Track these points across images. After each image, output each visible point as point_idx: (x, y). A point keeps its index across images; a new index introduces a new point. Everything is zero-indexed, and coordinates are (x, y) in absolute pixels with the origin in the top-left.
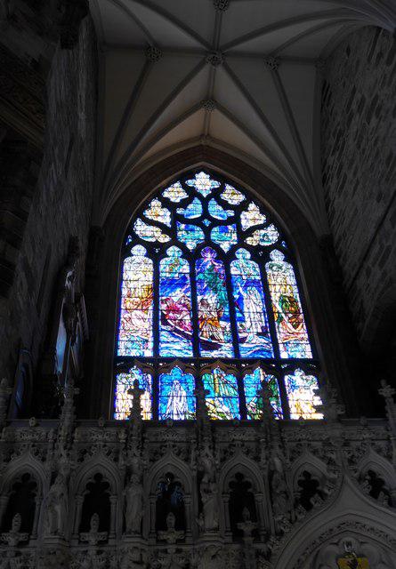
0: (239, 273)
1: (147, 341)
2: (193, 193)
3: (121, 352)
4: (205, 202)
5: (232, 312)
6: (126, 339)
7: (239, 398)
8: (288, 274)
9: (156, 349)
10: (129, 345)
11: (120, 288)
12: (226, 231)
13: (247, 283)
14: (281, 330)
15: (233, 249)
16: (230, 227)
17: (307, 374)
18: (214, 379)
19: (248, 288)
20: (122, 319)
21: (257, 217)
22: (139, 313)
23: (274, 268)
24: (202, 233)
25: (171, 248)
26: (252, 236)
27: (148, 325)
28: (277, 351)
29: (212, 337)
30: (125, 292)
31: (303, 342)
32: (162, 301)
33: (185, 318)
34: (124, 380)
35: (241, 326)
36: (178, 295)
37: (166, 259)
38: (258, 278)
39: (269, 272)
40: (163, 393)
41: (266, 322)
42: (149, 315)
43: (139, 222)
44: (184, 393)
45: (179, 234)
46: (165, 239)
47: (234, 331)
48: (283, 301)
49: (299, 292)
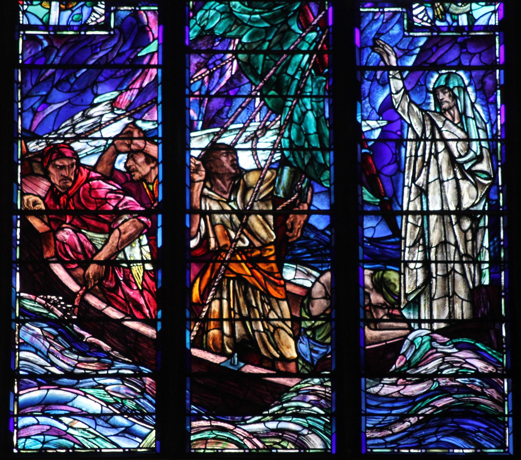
19: (433, 80)
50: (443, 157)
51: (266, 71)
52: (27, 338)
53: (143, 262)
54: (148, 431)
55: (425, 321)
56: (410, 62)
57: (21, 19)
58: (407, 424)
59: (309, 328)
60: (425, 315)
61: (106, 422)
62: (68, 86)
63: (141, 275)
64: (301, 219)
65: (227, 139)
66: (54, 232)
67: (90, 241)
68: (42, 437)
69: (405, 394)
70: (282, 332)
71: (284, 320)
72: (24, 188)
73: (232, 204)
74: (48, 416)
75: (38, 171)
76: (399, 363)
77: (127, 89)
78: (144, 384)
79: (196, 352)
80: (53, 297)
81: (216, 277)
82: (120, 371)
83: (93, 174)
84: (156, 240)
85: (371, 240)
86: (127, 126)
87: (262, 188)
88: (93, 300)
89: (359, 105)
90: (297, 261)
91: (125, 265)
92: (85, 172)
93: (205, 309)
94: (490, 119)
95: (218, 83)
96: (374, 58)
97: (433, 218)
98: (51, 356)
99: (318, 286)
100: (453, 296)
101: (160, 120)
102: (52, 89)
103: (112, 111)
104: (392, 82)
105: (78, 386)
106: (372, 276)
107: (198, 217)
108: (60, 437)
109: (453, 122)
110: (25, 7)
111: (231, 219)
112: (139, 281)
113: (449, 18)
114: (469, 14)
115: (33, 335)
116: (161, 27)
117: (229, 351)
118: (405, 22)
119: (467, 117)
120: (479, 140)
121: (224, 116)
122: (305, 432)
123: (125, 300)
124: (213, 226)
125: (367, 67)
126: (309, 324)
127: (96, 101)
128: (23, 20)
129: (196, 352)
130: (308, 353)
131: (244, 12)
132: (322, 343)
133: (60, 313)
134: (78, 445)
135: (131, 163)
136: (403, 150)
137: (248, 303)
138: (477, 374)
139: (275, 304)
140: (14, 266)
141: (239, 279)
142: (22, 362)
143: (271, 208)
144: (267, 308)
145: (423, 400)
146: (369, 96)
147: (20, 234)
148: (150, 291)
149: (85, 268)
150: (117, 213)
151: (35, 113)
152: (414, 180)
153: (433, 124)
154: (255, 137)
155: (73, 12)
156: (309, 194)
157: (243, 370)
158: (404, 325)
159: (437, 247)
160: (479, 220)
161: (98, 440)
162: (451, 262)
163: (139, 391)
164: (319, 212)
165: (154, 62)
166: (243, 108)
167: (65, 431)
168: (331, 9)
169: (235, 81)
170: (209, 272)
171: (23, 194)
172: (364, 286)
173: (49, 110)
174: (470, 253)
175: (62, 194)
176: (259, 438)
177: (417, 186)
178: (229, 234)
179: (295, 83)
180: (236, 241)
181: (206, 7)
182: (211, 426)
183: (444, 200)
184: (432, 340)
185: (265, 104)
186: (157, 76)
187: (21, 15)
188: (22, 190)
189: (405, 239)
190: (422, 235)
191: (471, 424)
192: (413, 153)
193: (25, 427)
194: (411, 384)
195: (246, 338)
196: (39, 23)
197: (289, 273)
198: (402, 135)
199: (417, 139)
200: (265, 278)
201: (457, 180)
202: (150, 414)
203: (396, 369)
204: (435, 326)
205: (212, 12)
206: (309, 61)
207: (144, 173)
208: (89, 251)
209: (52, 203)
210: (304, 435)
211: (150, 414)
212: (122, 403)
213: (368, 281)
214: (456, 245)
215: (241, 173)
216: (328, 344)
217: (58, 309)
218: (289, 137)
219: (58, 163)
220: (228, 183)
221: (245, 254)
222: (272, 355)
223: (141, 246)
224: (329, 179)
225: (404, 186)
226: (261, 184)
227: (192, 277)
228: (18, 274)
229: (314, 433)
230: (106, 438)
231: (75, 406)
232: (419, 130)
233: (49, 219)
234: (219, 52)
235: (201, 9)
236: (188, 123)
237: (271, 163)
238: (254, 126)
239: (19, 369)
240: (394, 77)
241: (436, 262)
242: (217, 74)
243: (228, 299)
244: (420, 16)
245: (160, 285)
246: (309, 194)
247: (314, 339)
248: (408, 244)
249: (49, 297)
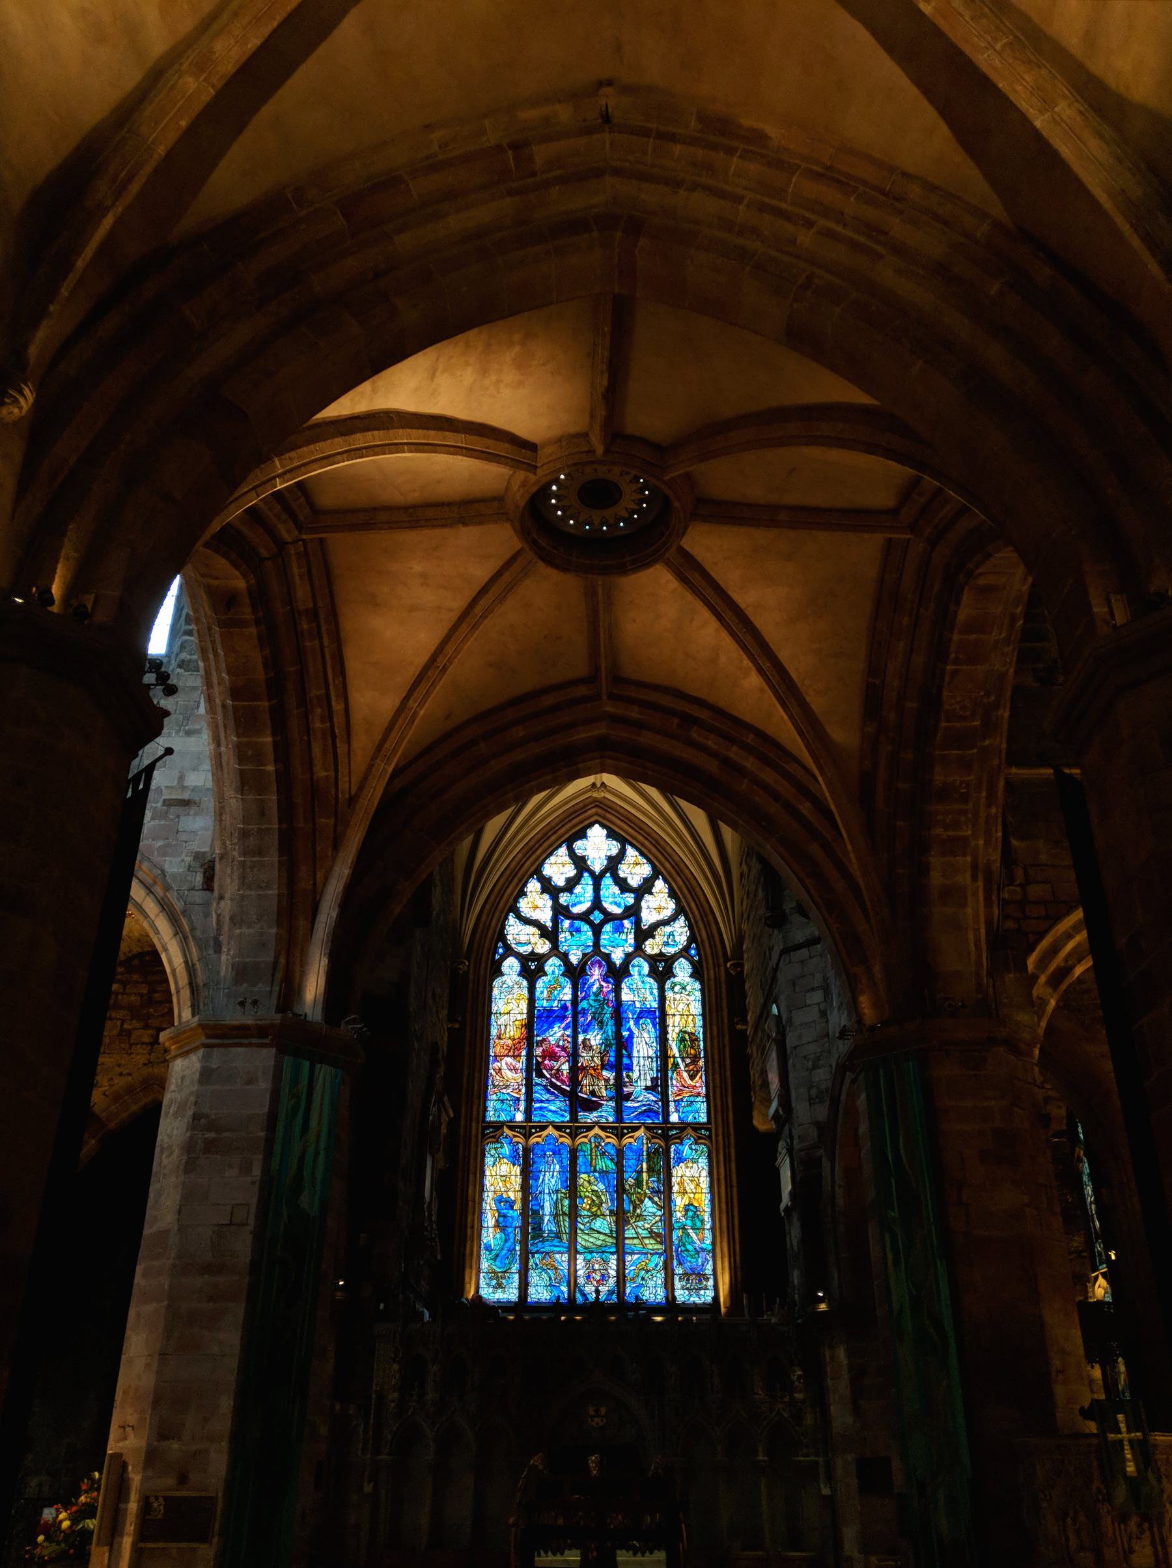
1: (518, 1099)
2: (580, 863)
3: (491, 1116)
4: (597, 880)
5: (619, 1057)
6: (494, 1097)
7: (617, 1173)
8: (692, 998)
9: (528, 1112)
10: (499, 1105)
11: (489, 1025)
12: (619, 929)
13: (641, 1012)
14: (674, 1082)
15: (628, 958)
16: (626, 923)
17: (696, 1143)
18: (591, 1150)
19: (641, 1022)
20: (491, 1071)
21: (663, 904)
22: (509, 1060)
23: (677, 989)
24: (590, 933)
25: (550, 962)
26: (653, 937)
27: (520, 1077)
28: (666, 1114)
29: (593, 1093)
30: (494, 1032)
31: (699, 1099)
32: (538, 1042)
34: (493, 1152)
35: (628, 1076)
36: (556, 1034)
38: (655, 1005)
39: (669, 994)
40: (533, 1168)
41: (657, 1070)
42: (521, 1064)
43: (512, 919)
44: (557, 1167)
45: (562, 937)
46: (543, 947)
47: (619, 1084)
48: (682, 1040)
49: (704, 1027)
50: (644, 1042)
56: (635, 1016)
65: (588, 1037)
66: (543, 1062)
76: (633, 1097)
79: (580, 1094)
85: (626, 1064)
90: (606, 1069)
129: (580, 1094)
141: (591, 1074)
150: (560, 1057)
151: (539, 1029)
154: (595, 1036)
191: (651, 1114)
215: (591, 1046)
238: (595, 1033)
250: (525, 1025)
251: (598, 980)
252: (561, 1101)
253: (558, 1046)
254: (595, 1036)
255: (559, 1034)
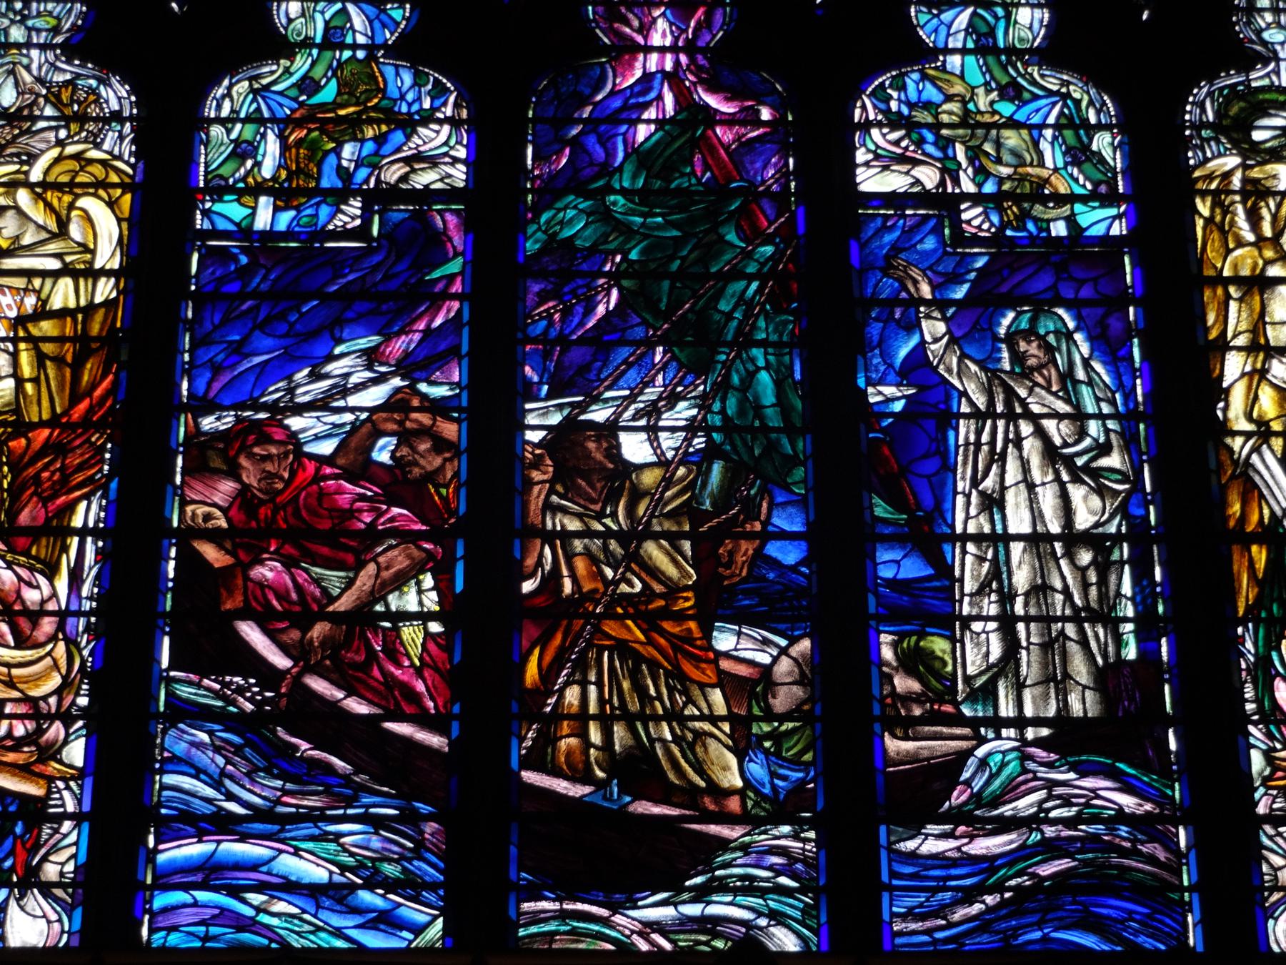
0: (929, 177)
32: (199, 445)
33: (408, 600)
35: (914, 661)
37: (269, 71)
41: (1147, 629)
50: (1031, 447)
51: (675, 304)
52: (180, 748)
53: (424, 617)
54: (428, 918)
55: (1008, 723)
56: (960, 292)
57: (199, 222)
58: (977, 908)
59: (767, 736)
60: (1006, 709)
61: (340, 901)
62: (284, 328)
63: (419, 642)
64: (747, 547)
65: (599, 414)
67: (317, 581)
68: (203, 929)
69: (973, 852)
70: (710, 741)
71: (714, 719)
72: (188, 492)
73: (608, 521)
74: (216, 889)
75: (217, 463)
76: (958, 797)
77: (398, 334)
78: (422, 833)
79: (530, 776)
80: (236, 679)
81: (574, 644)
82: (372, 810)
83: (328, 470)
84: (452, 580)
85: (893, 583)
86: (398, 390)
87: (668, 494)
88: (318, 685)
89: (861, 362)
90: (742, 618)
91: (387, 624)
92: (311, 467)
93: (552, 701)
94: (1120, 386)
95: (582, 324)
96: (887, 287)
97: (1017, 548)
98: (228, 783)
99: (784, 659)
100: (1063, 681)
101: (464, 382)
102: (252, 331)
103: (369, 367)
104: (925, 324)
105: (283, 835)
106: (895, 645)
107: (538, 542)
108: (240, 929)
109: (1048, 390)
110: (208, 205)
111: (605, 548)
112: (415, 652)
113: (1031, 226)
114: (1071, 220)
115: (193, 744)
116: (471, 237)
117: (600, 774)
118: (947, 231)
119: (1076, 382)
120: (1100, 416)
121: (592, 376)
122: (763, 922)
123: (386, 684)
124: (570, 558)
125: (874, 301)
126: (766, 728)
127: (337, 351)
128: (200, 222)
129: (530, 776)
130: (766, 779)
131: (634, 213)
132: (795, 763)
133: (249, 707)
134: (277, 943)
135: (405, 451)
136: (951, 434)
137: (640, 689)
138: (1121, 816)
139: (696, 692)
140: (160, 622)
141: (622, 648)
142: (166, 793)
143: (687, 528)
144: (680, 700)
145: (1010, 865)
146: (879, 345)
147: (175, 569)
148: (436, 669)
149: (306, 629)
150: (373, 536)
151: (217, 370)
152: (975, 483)
153: (1010, 394)
154: (653, 410)
155: (299, 212)
156: (765, 505)
157: (631, 809)
158: (966, 731)
159: (1027, 594)
160: (1110, 551)
161: (323, 935)
162: (1056, 619)
163: (410, 845)
164: (783, 535)
165: (457, 287)
166: (630, 365)
167: (252, 919)
168: (801, 211)
169: (615, 320)
170: (558, 640)
171: (184, 503)
172: (881, 663)
173: (246, 365)
174: (1094, 605)
175: (262, 502)
176: (664, 934)
177: (982, 494)
178: (601, 573)
179: (735, 323)
180: (616, 583)
181: (559, 205)
182: (562, 911)
183: (1036, 515)
184: (1025, 757)
185: (674, 358)
186: (459, 312)
187: (199, 217)
188: (183, 497)
189: (961, 580)
190: (995, 573)
191: (1111, 908)
192: (972, 438)
193: (167, 910)
194: (985, 835)
195: (637, 752)
196: (231, 227)
197: (724, 640)
198: (949, 407)
199: (977, 415)
200: (676, 649)
201: (1062, 485)
202: (433, 887)
203: (951, 808)
204: (1030, 733)
205: (570, 213)
206: (759, 291)
207: (429, 468)
208: (314, 598)
209: (243, 517)
210: (761, 928)
211: (433, 887)
212: (374, 867)
213: (887, 653)
214: (1066, 591)
216: (807, 764)
217: (247, 699)
218: (723, 411)
219: (257, 450)
220: (599, 485)
221: (635, 606)
222: (690, 782)
223: (420, 592)
224: (804, 481)
225: (955, 493)
226: (666, 489)
227: (525, 643)
228: (166, 641)
229: (779, 923)
230: (338, 933)
231: (274, 872)
232: (981, 401)
233: (235, 546)
234: (583, 274)
235: (549, 207)
236: (520, 387)
237: (686, 453)
238: (651, 394)
239: (160, 805)
240: (928, 317)
241: (1027, 619)
242: (580, 309)
243: (599, 684)
244: (976, 223)
245: (457, 658)
246: (765, 505)
247: (775, 754)
248: (967, 589)
249: (228, 678)
250: (110, 337)
251: (673, 79)
252: (377, 823)
253: (361, 468)
254: (653, 410)
255: (375, 396)
